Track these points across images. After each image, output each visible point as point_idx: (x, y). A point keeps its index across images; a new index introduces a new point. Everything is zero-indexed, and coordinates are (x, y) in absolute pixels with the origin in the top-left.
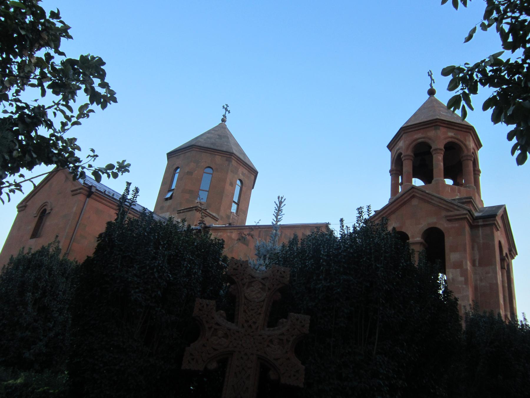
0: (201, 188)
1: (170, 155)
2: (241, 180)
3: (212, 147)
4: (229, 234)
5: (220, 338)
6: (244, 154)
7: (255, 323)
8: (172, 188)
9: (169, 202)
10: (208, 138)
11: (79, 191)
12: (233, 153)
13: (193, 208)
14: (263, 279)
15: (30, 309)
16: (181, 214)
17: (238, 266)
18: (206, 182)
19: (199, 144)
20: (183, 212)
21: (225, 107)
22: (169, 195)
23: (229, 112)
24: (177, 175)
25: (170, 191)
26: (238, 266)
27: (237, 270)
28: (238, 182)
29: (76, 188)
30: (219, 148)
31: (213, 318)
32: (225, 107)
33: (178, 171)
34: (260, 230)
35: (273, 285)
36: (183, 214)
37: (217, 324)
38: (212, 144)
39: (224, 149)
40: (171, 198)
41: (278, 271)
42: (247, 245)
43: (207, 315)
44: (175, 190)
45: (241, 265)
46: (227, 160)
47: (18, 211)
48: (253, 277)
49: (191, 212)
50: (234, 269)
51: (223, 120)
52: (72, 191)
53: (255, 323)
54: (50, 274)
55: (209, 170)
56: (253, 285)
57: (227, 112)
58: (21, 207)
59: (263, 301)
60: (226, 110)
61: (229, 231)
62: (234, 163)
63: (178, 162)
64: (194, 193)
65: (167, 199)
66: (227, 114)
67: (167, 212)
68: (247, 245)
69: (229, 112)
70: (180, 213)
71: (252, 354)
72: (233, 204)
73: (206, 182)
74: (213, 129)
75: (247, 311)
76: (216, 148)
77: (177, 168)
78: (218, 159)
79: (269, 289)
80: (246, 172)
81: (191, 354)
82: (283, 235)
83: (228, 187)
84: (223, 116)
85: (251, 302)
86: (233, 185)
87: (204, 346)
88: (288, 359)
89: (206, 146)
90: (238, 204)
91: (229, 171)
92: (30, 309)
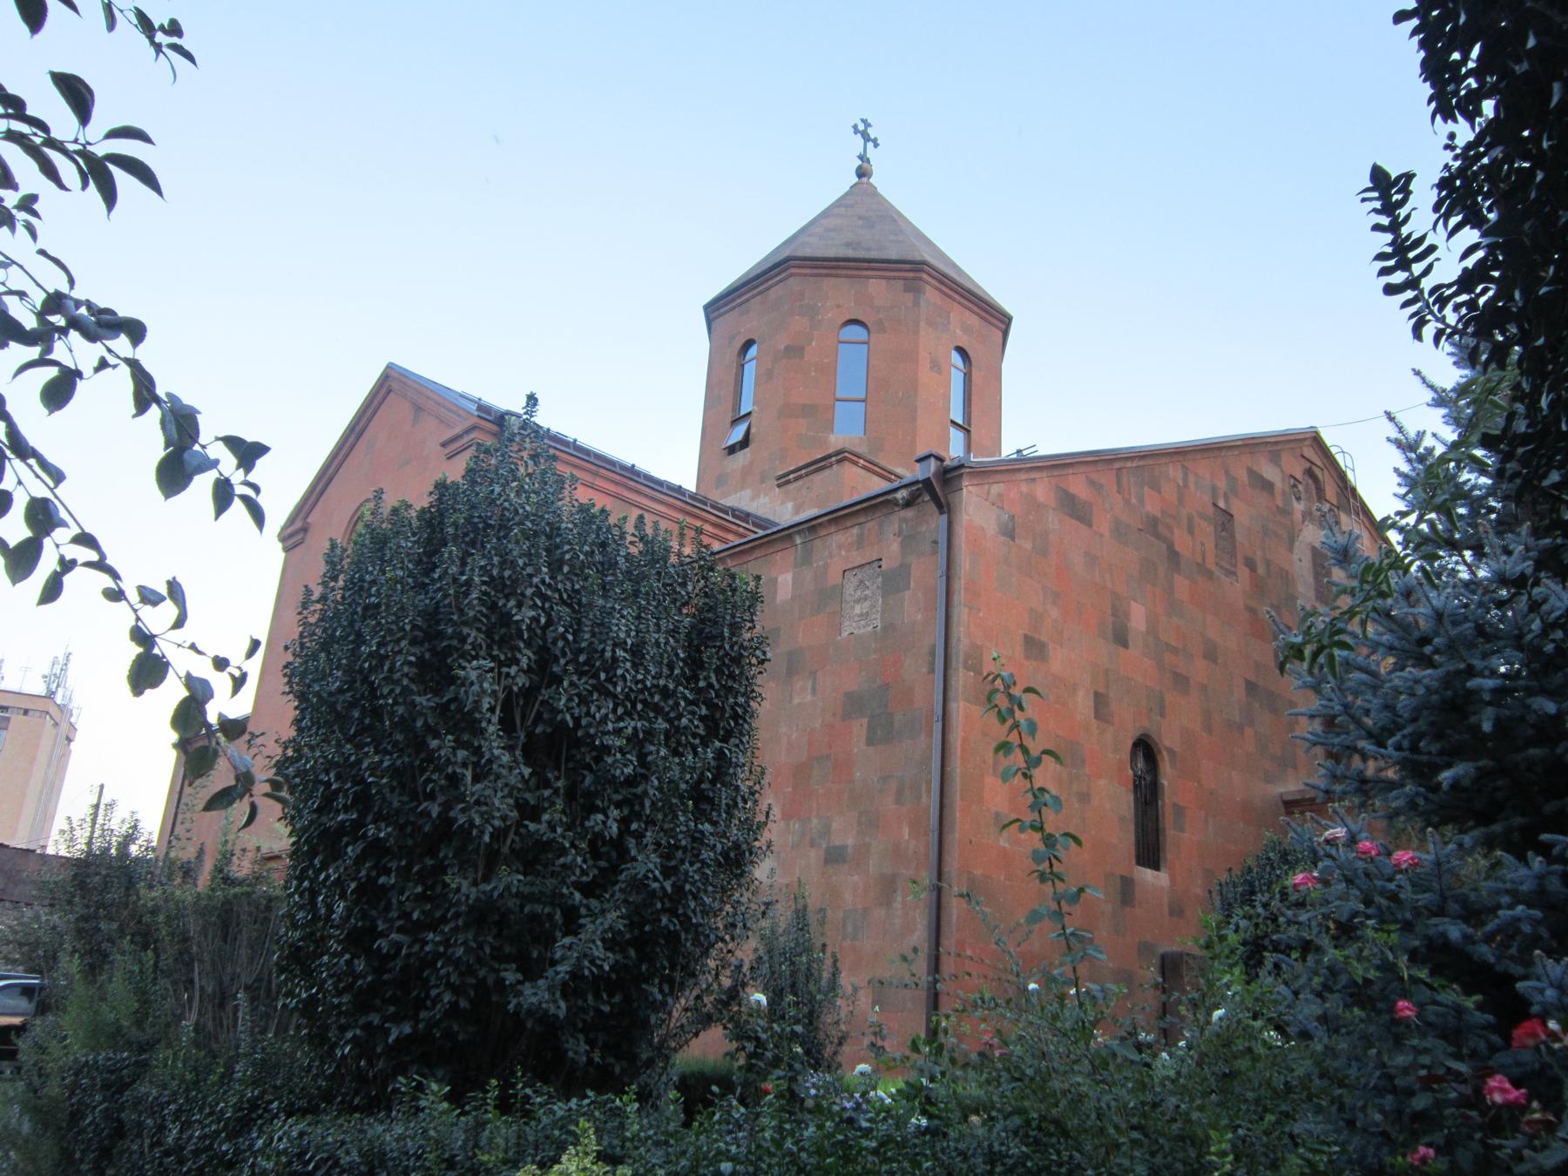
0: (839, 395)
1: (715, 310)
2: (961, 351)
3: (850, 253)
4: (1024, 488)
6: (955, 266)
8: (743, 413)
9: (742, 457)
10: (828, 230)
11: (466, 439)
12: (924, 263)
13: (830, 456)
15: (494, 744)
16: (791, 487)
18: (852, 368)
19: (808, 252)
20: (796, 479)
21: (861, 127)
22: (737, 434)
23: (876, 145)
24: (750, 370)
25: (735, 422)
28: (956, 358)
29: (457, 430)
30: (873, 255)
32: (861, 127)
33: (753, 351)
34: (1117, 465)
36: (800, 483)
38: (848, 245)
39: (893, 254)
40: (745, 443)
42: (1090, 526)
44: (753, 419)
46: (906, 290)
47: (287, 550)
49: (827, 473)
51: (862, 173)
52: (444, 445)
54: (555, 566)
55: (855, 332)
57: (870, 145)
58: (291, 535)
60: (866, 137)
61: (1023, 476)
62: (931, 295)
63: (748, 322)
64: (820, 414)
65: (732, 450)
66: (871, 152)
67: (742, 488)
68: (1090, 526)
69: (876, 145)
70: (788, 482)
72: (952, 430)
73: (852, 368)
74: (839, 203)
76: (862, 254)
77: (749, 344)
78: (878, 289)
80: (974, 321)
82: (1191, 478)
83: (925, 374)
84: (861, 158)
86: (938, 367)
89: (831, 253)
90: (965, 430)
91: (922, 324)
92: (494, 744)
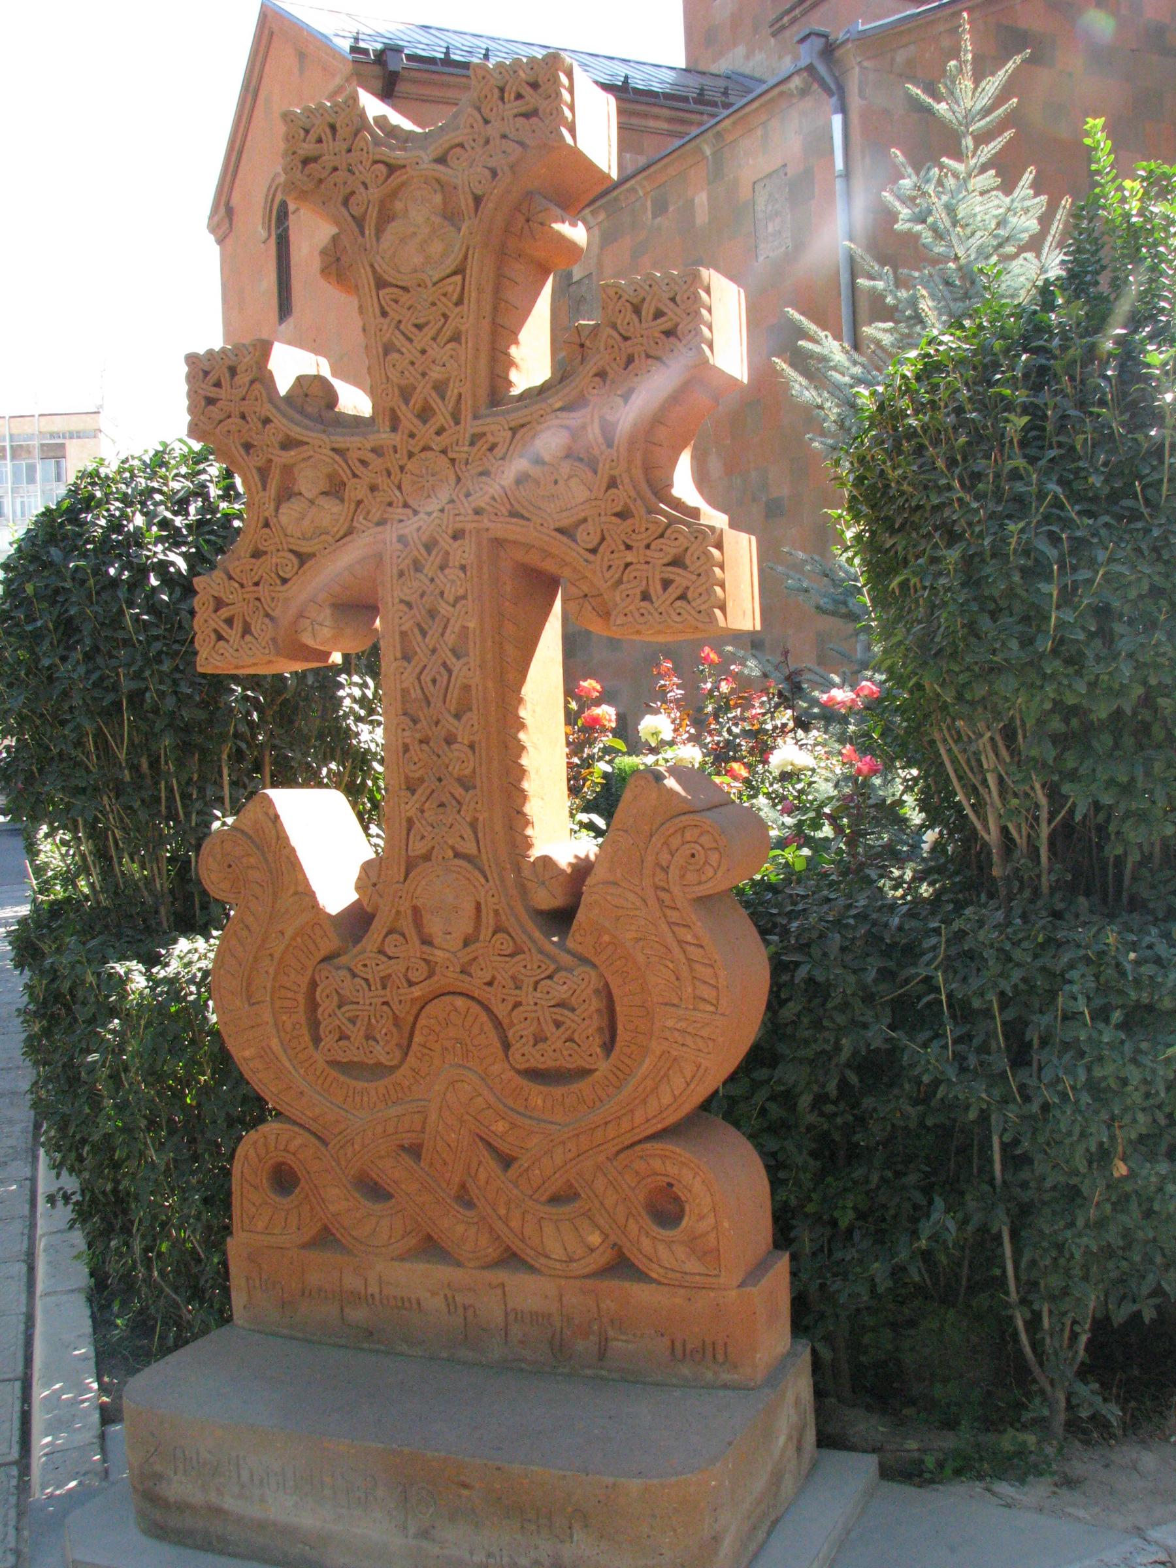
5: (312, 502)
7: (440, 388)
14: (441, 160)
17: (320, 141)
26: (320, 141)
27: (315, 159)
31: (266, 421)
35: (494, 173)
37: (288, 444)
41: (502, 90)
43: (243, 417)
45: (333, 128)
48: (392, 169)
50: (306, 162)
53: (440, 388)
56: (399, 205)
59: (460, 271)
71: (457, 536)
75: (399, 341)
79: (478, 200)
81: (219, 604)
85: (405, 289)
87: (257, 554)
88: (623, 515)
